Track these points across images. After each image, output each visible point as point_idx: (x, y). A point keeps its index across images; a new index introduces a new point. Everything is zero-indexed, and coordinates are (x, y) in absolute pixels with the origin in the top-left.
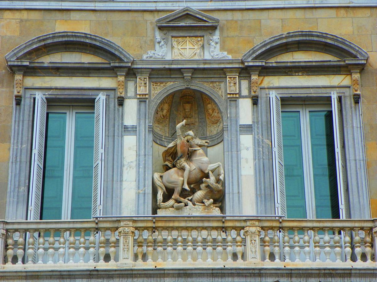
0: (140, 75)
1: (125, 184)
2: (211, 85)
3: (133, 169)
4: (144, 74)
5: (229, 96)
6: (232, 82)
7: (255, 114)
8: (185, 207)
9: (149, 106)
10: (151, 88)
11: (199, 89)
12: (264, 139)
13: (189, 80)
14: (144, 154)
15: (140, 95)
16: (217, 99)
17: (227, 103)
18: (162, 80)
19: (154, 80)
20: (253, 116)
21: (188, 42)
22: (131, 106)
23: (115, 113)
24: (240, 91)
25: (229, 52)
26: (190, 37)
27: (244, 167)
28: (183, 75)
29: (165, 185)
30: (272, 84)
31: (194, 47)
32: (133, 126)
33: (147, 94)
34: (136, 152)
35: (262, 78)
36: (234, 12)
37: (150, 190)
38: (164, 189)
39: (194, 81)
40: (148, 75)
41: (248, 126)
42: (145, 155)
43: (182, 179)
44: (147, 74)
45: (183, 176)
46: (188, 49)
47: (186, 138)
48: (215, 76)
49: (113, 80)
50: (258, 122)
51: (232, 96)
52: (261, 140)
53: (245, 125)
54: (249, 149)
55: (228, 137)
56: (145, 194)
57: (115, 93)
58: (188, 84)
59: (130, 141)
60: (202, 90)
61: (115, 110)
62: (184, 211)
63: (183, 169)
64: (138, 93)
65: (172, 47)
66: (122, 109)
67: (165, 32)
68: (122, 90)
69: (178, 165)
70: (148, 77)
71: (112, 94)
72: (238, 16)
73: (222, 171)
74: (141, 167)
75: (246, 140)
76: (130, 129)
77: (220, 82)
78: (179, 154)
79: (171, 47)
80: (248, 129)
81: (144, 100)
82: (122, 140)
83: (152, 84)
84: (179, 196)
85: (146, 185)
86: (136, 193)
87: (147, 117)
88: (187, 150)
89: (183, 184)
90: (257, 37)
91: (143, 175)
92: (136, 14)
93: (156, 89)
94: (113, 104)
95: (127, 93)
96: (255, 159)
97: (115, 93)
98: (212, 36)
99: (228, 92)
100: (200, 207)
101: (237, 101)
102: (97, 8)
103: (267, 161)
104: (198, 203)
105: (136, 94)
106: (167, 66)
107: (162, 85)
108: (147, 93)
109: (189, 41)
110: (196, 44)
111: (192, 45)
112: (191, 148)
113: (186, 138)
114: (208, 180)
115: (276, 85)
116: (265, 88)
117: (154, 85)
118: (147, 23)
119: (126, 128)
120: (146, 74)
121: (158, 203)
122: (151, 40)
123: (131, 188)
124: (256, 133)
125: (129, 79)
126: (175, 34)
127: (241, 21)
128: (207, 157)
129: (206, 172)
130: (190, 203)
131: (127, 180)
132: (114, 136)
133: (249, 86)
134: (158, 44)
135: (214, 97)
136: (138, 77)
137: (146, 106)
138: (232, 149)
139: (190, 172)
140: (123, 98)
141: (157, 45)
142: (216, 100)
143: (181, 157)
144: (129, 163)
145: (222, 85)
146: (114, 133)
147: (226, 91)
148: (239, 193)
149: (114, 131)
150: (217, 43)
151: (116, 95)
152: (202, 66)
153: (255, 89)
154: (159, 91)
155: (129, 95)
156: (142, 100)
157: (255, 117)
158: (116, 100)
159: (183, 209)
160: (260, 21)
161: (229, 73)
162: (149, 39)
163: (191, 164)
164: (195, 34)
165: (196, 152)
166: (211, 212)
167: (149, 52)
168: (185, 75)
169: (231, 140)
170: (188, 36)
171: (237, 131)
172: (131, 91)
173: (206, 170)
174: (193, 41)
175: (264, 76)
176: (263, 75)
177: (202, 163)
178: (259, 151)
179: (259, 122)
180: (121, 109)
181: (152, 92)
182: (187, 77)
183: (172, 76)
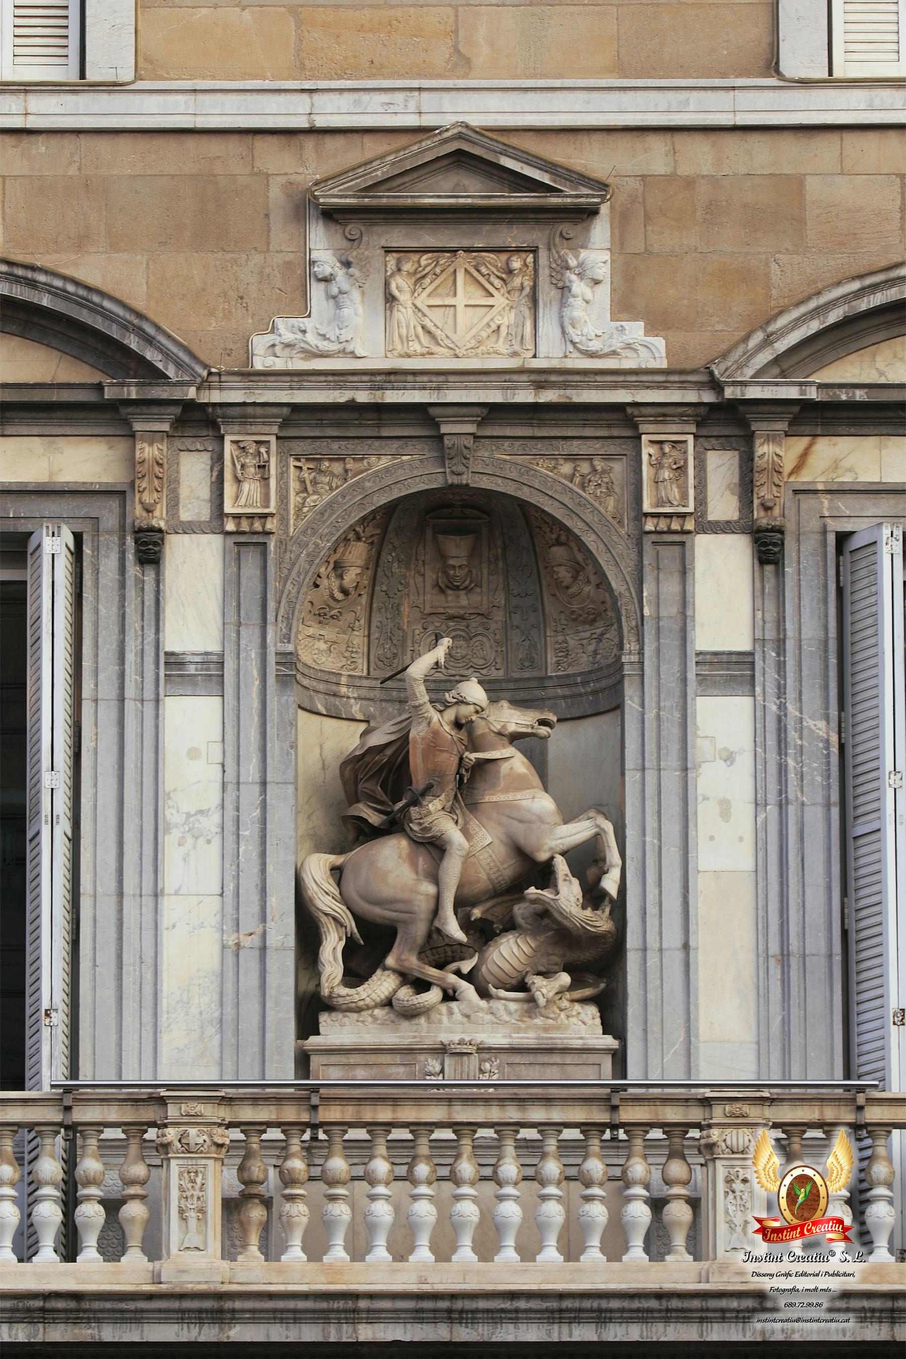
0: (237, 428)
1: (172, 910)
2: (566, 468)
3: (209, 842)
4: (256, 423)
5: (649, 526)
6: (667, 461)
7: (770, 606)
8: (443, 1008)
9: (279, 564)
10: (287, 484)
11: (509, 489)
12: (805, 716)
13: (465, 452)
14: (258, 780)
15: (237, 517)
16: (593, 537)
17: (640, 553)
18: (335, 446)
19: (298, 447)
20: (759, 614)
21: (460, 276)
22: (195, 567)
23: (123, 598)
24: (701, 501)
25: (657, 323)
26: (468, 250)
27: (712, 838)
28: (439, 429)
29: (355, 908)
30: (850, 470)
31: (489, 301)
32: (207, 654)
33: (272, 515)
34: (220, 767)
35: (806, 440)
36: (680, 140)
37: (283, 932)
38: (351, 924)
39: (486, 454)
40: (275, 429)
41: (734, 658)
42: (264, 783)
43: (431, 889)
44: (270, 424)
45: (435, 878)
46: (460, 309)
47: (450, 714)
48: (588, 432)
49: (110, 448)
50: (780, 644)
51: (663, 525)
52: (791, 724)
53: (723, 653)
54: (738, 759)
55: (643, 705)
56: (263, 949)
57: (123, 506)
58: (461, 468)
59: (192, 723)
60: (524, 494)
61: (122, 585)
62: (440, 1022)
63: (435, 847)
64: (228, 508)
65: (390, 299)
66: (158, 582)
67: (353, 228)
68: (155, 495)
69: (416, 828)
70: (273, 439)
71: (110, 511)
72: (699, 157)
73: (613, 855)
74: (244, 833)
75: (725, 721)
76: (192, 670)
77: (608, 457)
78: (419, 780)
79: (381, 300)
80: (732, 671)
81: (255, 539)
82: (157, 716)
83: (292, 463)
84: (420, 958)
85: (269, 917)
86: (224, 947)
87: (271, 617)
88: (455, 761)
89: (436, 911)
90: (784, 258)
91: (256, 870)
92: (215, 146)
93: (310, 489)
94: (114, 556)
95: (177, 504)
96: (759, 804)
97: (123, 506)
98: (575, 249)
99: (647, 507)
100: (513, 1006)
101: (688, 545)
102: (32, 123)
103: (819, 811)
104: (502, 993)
105: (219, 513)
106: (363, 397)
107: (337, 468)
108: (272, 509)
109: (466, 270)
110: (497, 283)
111: (481, 292)
112: (475, 750)
113: (450, 714)
114: (547, 894)
115: (869, 476)
116: (816, 492)
117: (300, 468)
118: (268, 185)
119: (174, 661)
120: (264, 423)
121: (325, 992)
122: (288, 265)
123: (202, 925)
124: (771, 690)
125: (188, 443)
126: (398, 236)
127: (713, 180)
128: (546, 790)
129: (543, 856)
130: (468, 990)
131: (181, 892)
132: (122, 700)
133: (742, 476)
134: (322, 285)
135: (581, 525)
136: (228, 439)
137: (264, 568)
138: (659, 758)
139: (468, 858)
140: (160, 531)
141: (317, 292)
142: (589, 540)
143: (428, 790)
144: (189, 815)
145: (618, 469)
146: (122, 688)
147: (639, 500)
148: (686, 947)
149: (122, 675)
150: (597, 282)
151: (129, 521)
152: (525, 396)
153: (764, 492)
154: (327, 498)
155: (185, 515)
156: (247, 539)
157: (770, 616)
158: (130, 541)
159: (434, 1016)
160: (797, 183)
161: (650, 422)
162: (278, 259)
163: (474, 824)
164: (497, 242)
165: (490, 766)
166: (558, 1028)
167: (280, 323)
168: (444, 429)
169: (658, 716)
170: (461, 248)
171: (684, 680)
172: (198, 498)
173: (539, 851)
174: (484, 270)
175: (815, 436)
176: (807, 429)
177: (521, 821)
178: (782, 769)
179: (784, 640)
180: (149, 578)
181: (294, 500)
182: (455, 438)
183: (385, 432)
